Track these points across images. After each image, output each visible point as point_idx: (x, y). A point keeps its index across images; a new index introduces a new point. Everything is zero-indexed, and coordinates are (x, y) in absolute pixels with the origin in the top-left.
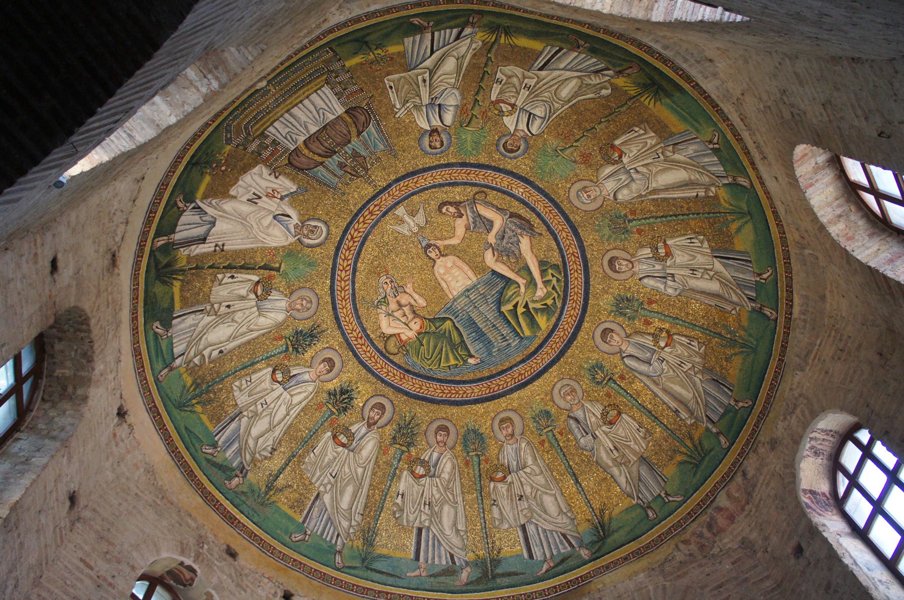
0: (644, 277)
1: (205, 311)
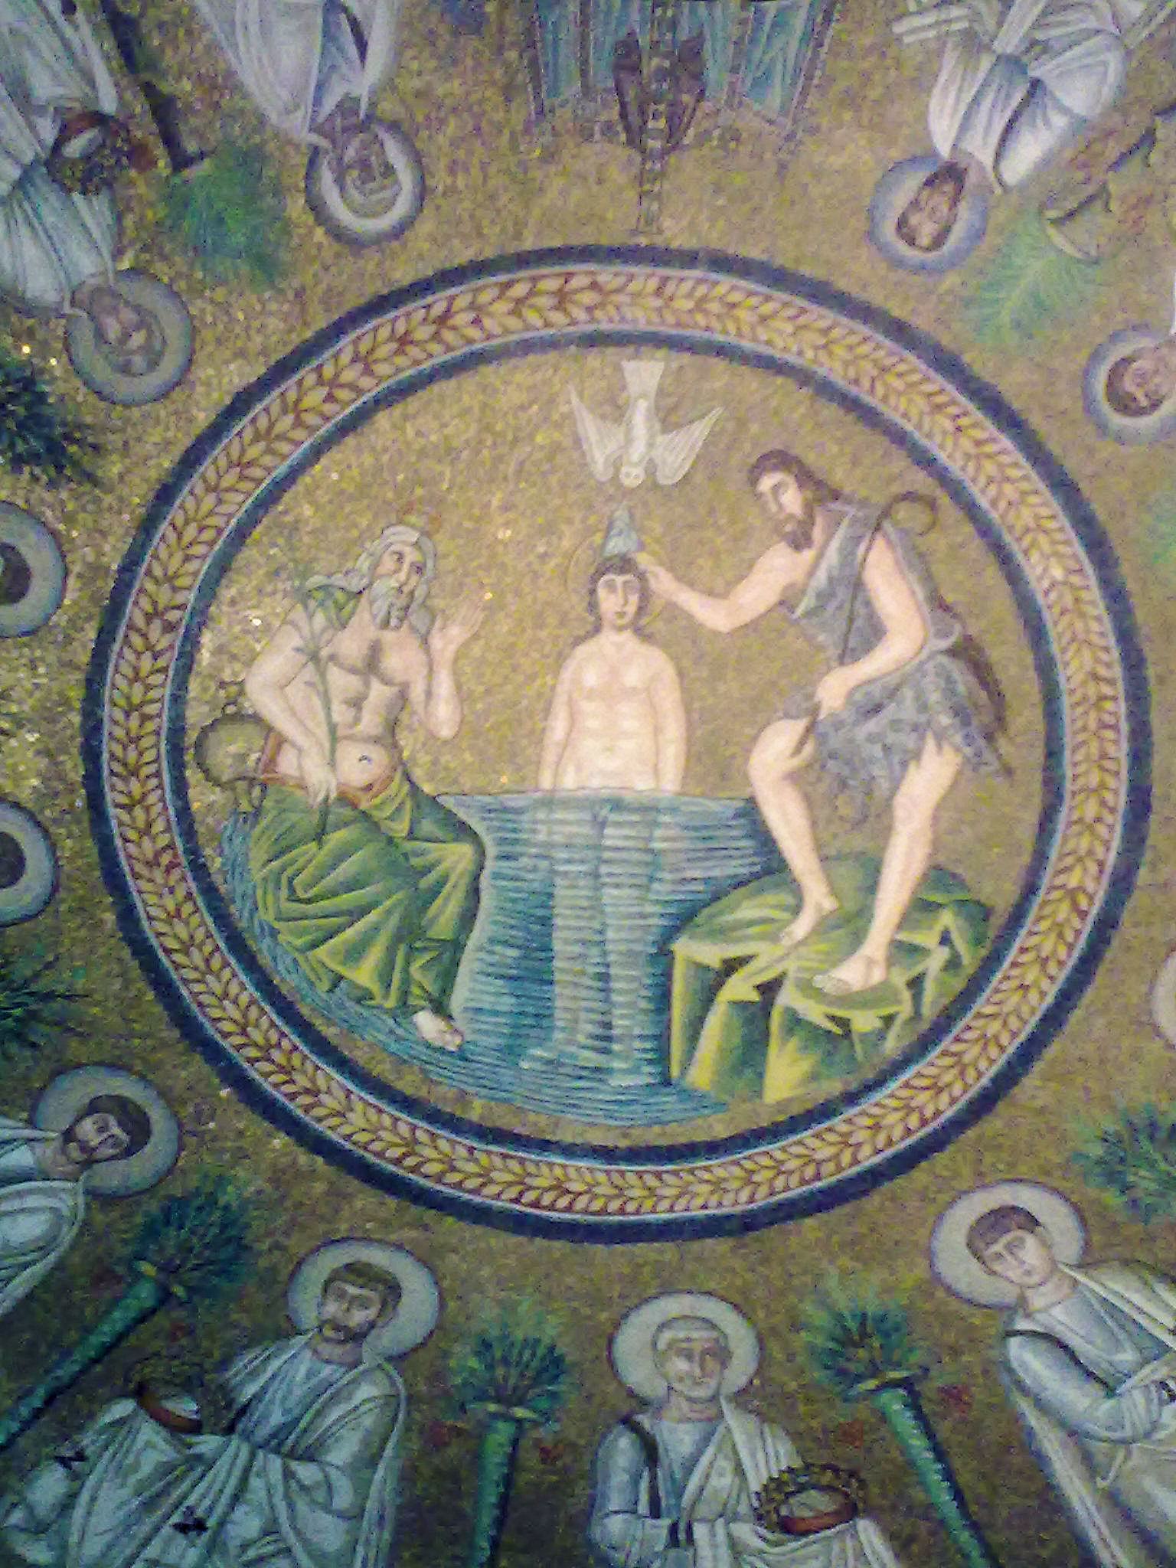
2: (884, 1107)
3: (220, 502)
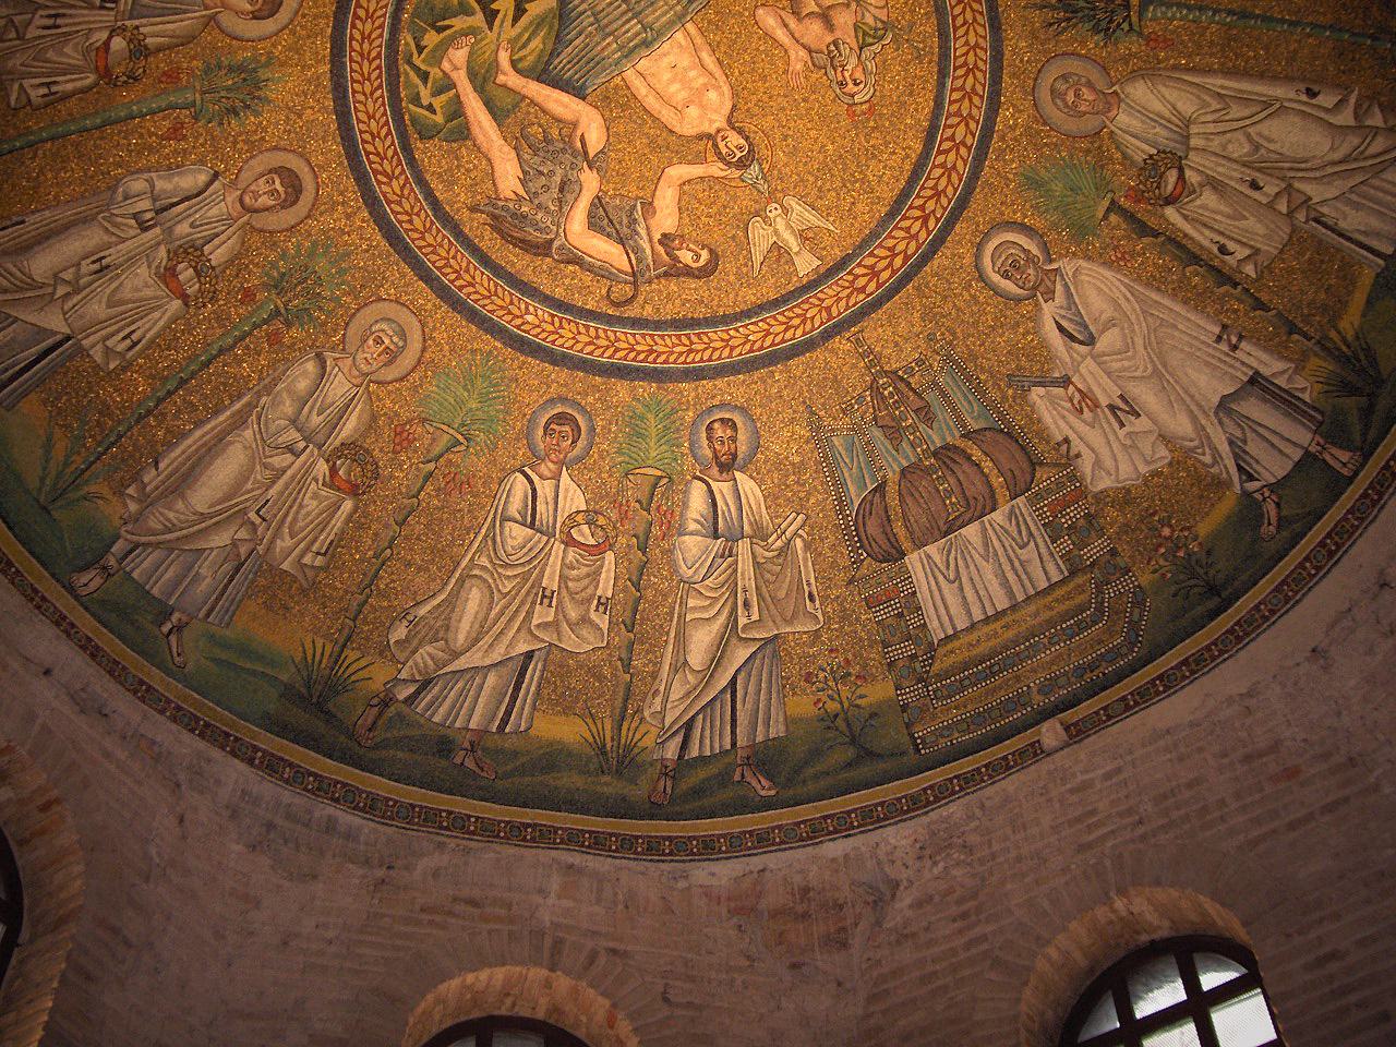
0: (211, 183)
1: (1313, 214)
2: (381, 8)
3: (967, 43)
